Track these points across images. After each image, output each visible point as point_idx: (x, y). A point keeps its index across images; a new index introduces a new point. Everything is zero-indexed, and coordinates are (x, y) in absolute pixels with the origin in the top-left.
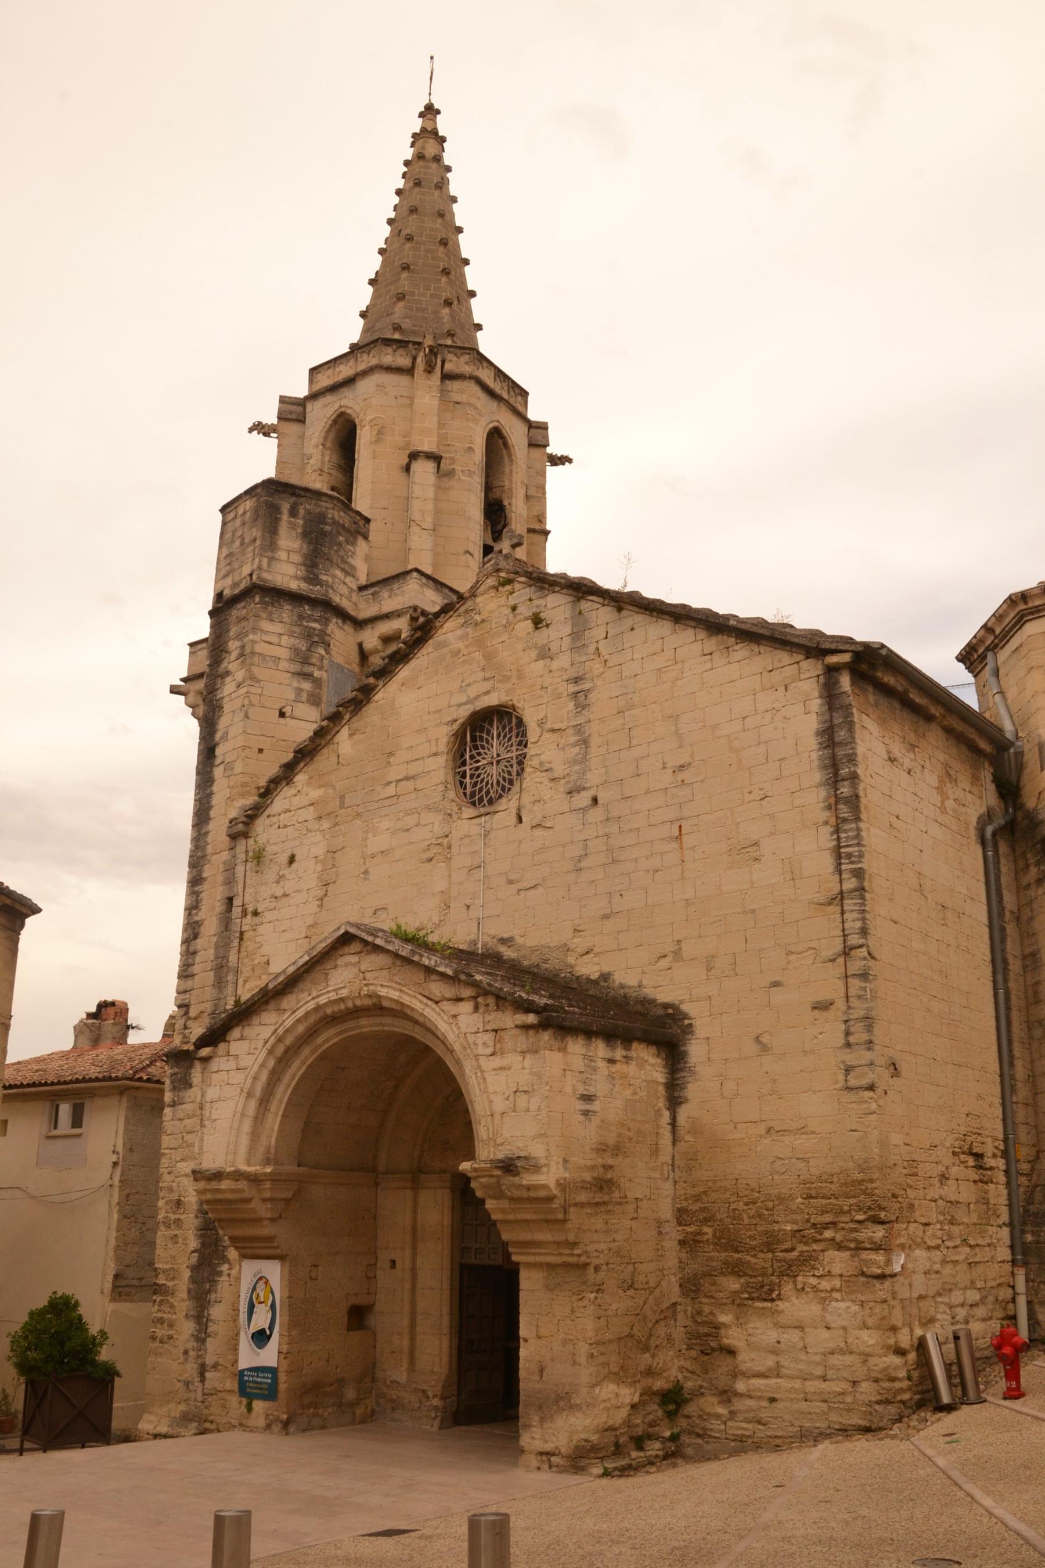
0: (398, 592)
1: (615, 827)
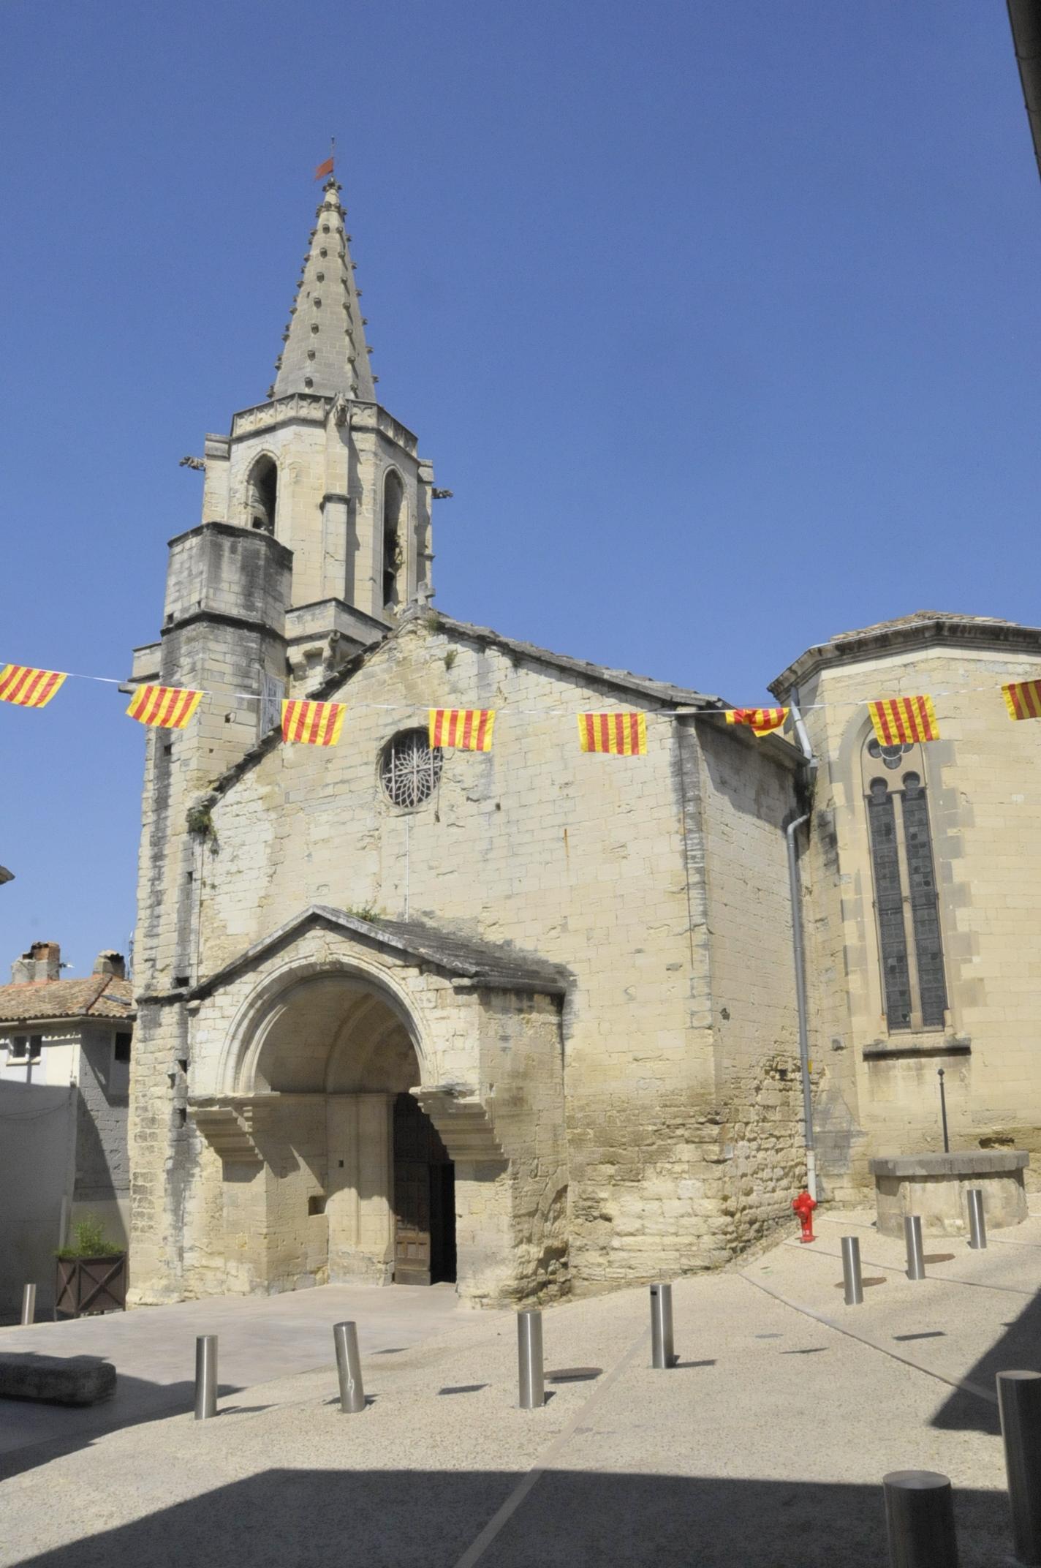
1: (514, 829)
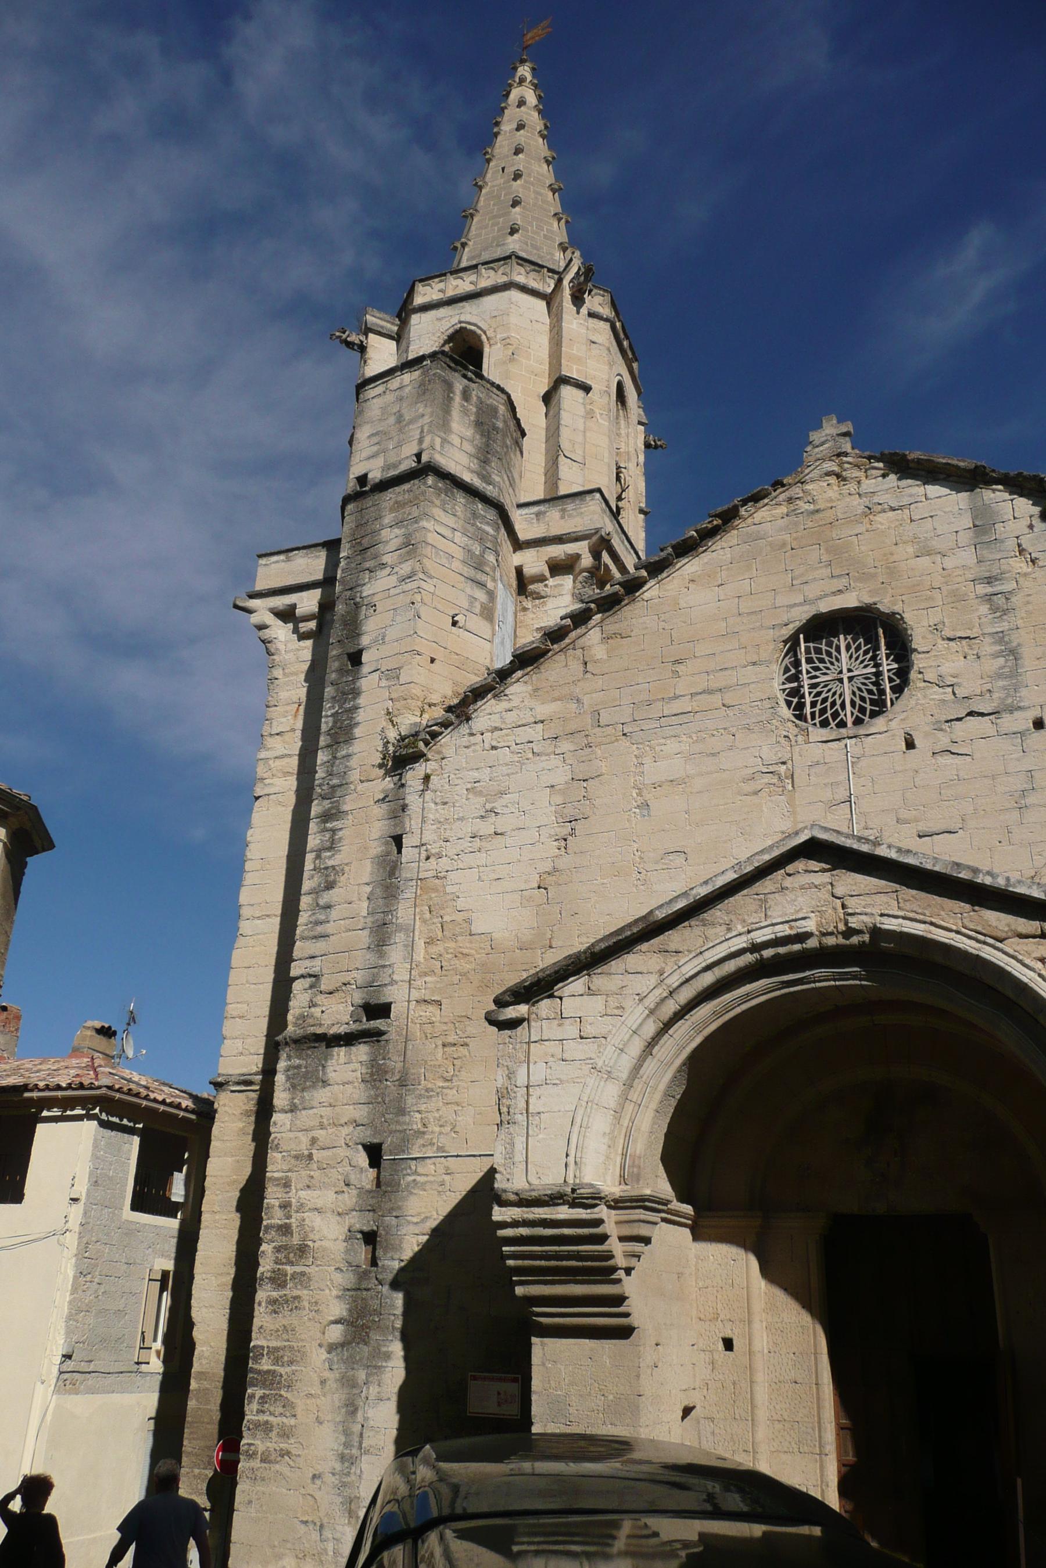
0: (574, 513)
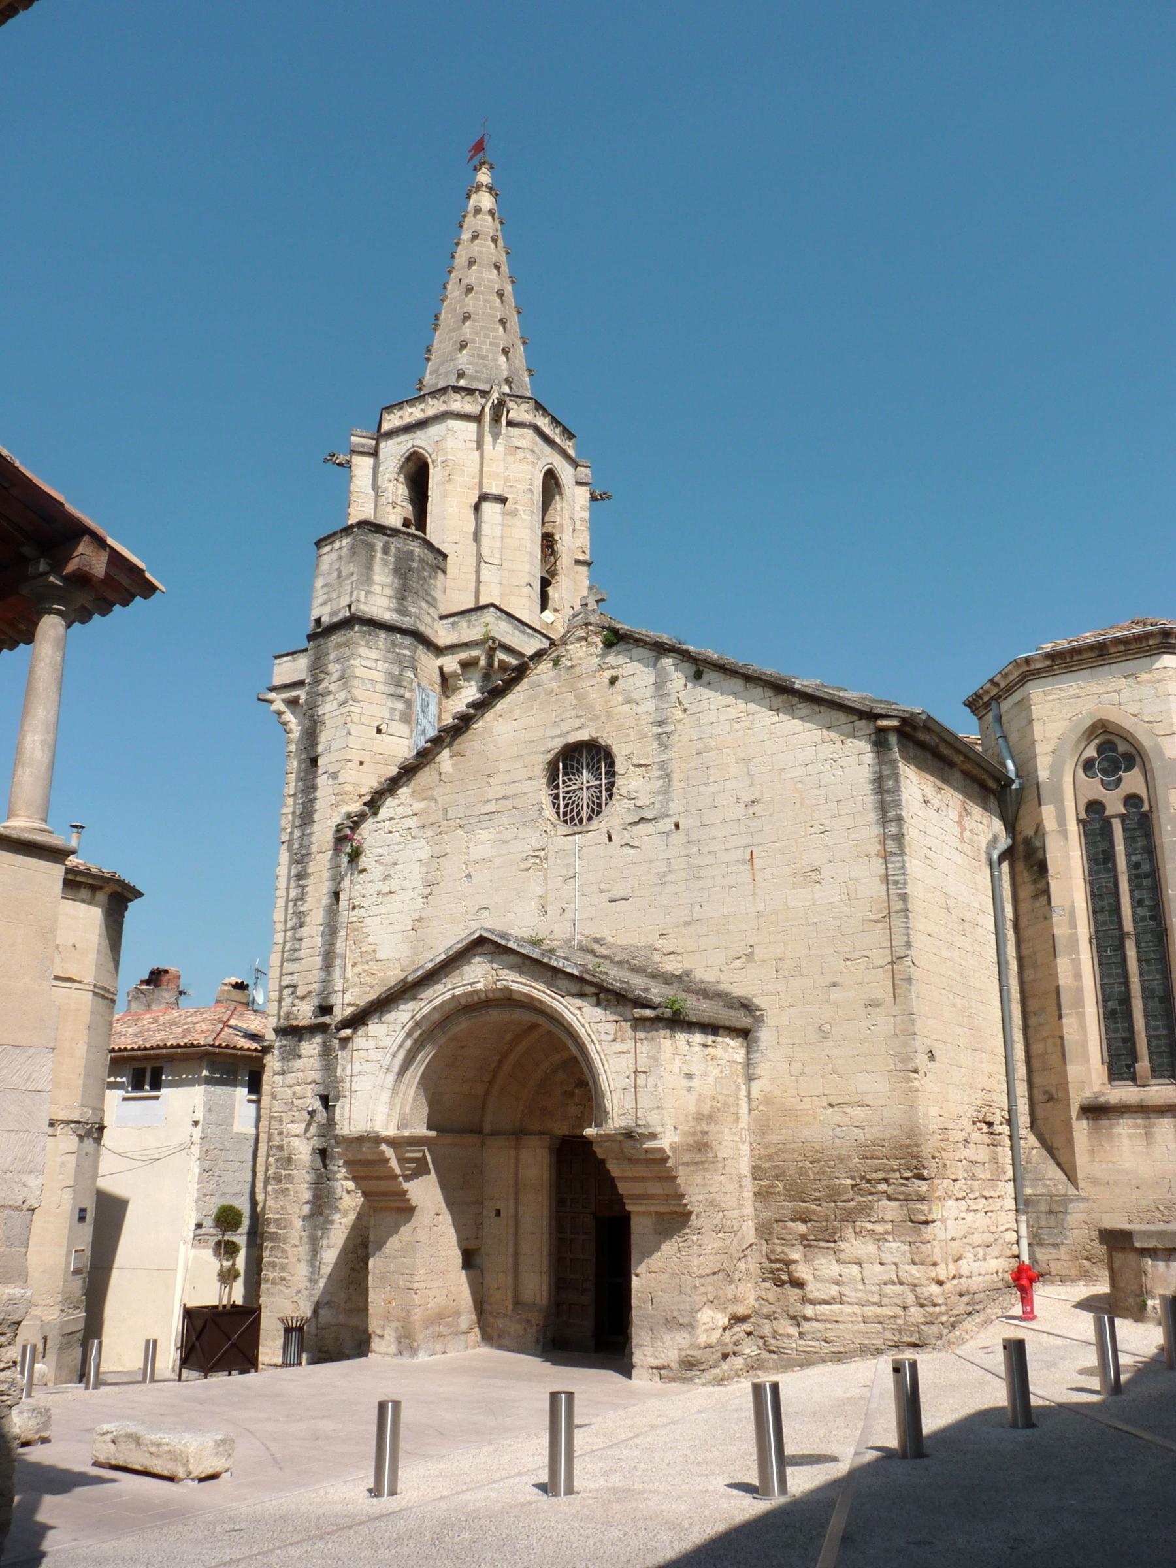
1: (696, 850)
